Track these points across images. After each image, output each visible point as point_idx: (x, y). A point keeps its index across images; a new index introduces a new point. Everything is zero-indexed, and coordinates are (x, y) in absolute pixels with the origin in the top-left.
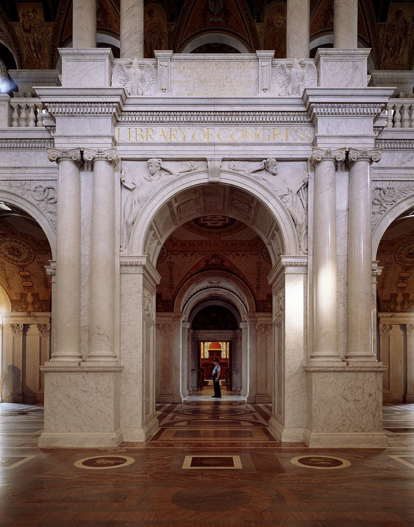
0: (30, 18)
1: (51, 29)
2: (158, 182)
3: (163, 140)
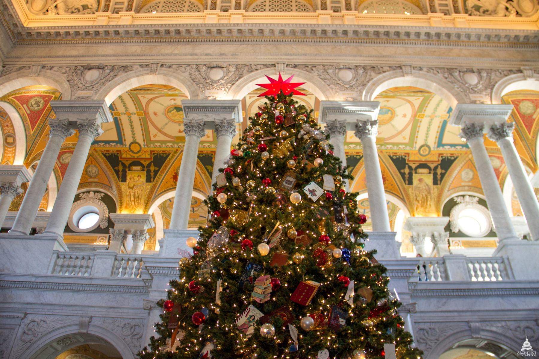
1: (149, 187)
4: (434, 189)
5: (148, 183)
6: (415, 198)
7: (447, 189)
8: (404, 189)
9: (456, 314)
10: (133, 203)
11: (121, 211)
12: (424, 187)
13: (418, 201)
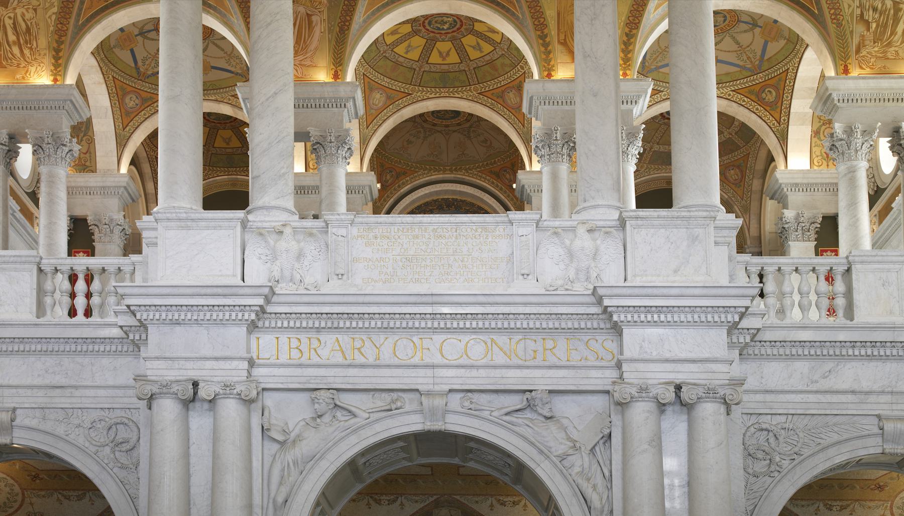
2: (331, 429)
3: (339, 359)
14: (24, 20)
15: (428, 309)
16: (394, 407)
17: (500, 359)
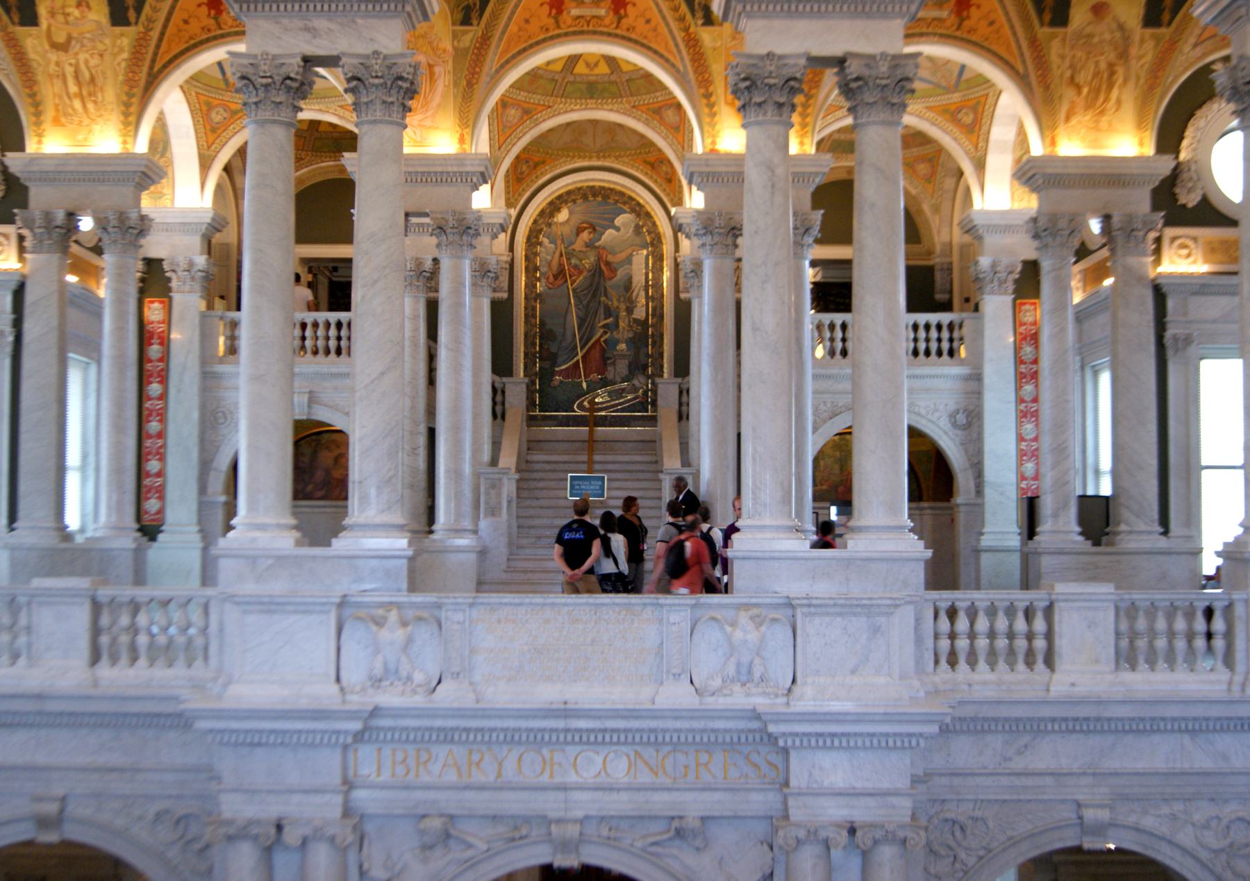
0: (71, 19)
1: (125, 42)
3: (452, 777)
4: (1142, 41)
5: (118, 30)
6: (1068, 74)
7: (1192, 40)
8: (1034, 42)
9: (1049, 780)
10: (77, 104)
11: (40, 142)
12: (1107, 36)
13: (1079, 88)
14: (88, 68)
15: (560, 724)
16: (517, 835)
17: (645, 777)
